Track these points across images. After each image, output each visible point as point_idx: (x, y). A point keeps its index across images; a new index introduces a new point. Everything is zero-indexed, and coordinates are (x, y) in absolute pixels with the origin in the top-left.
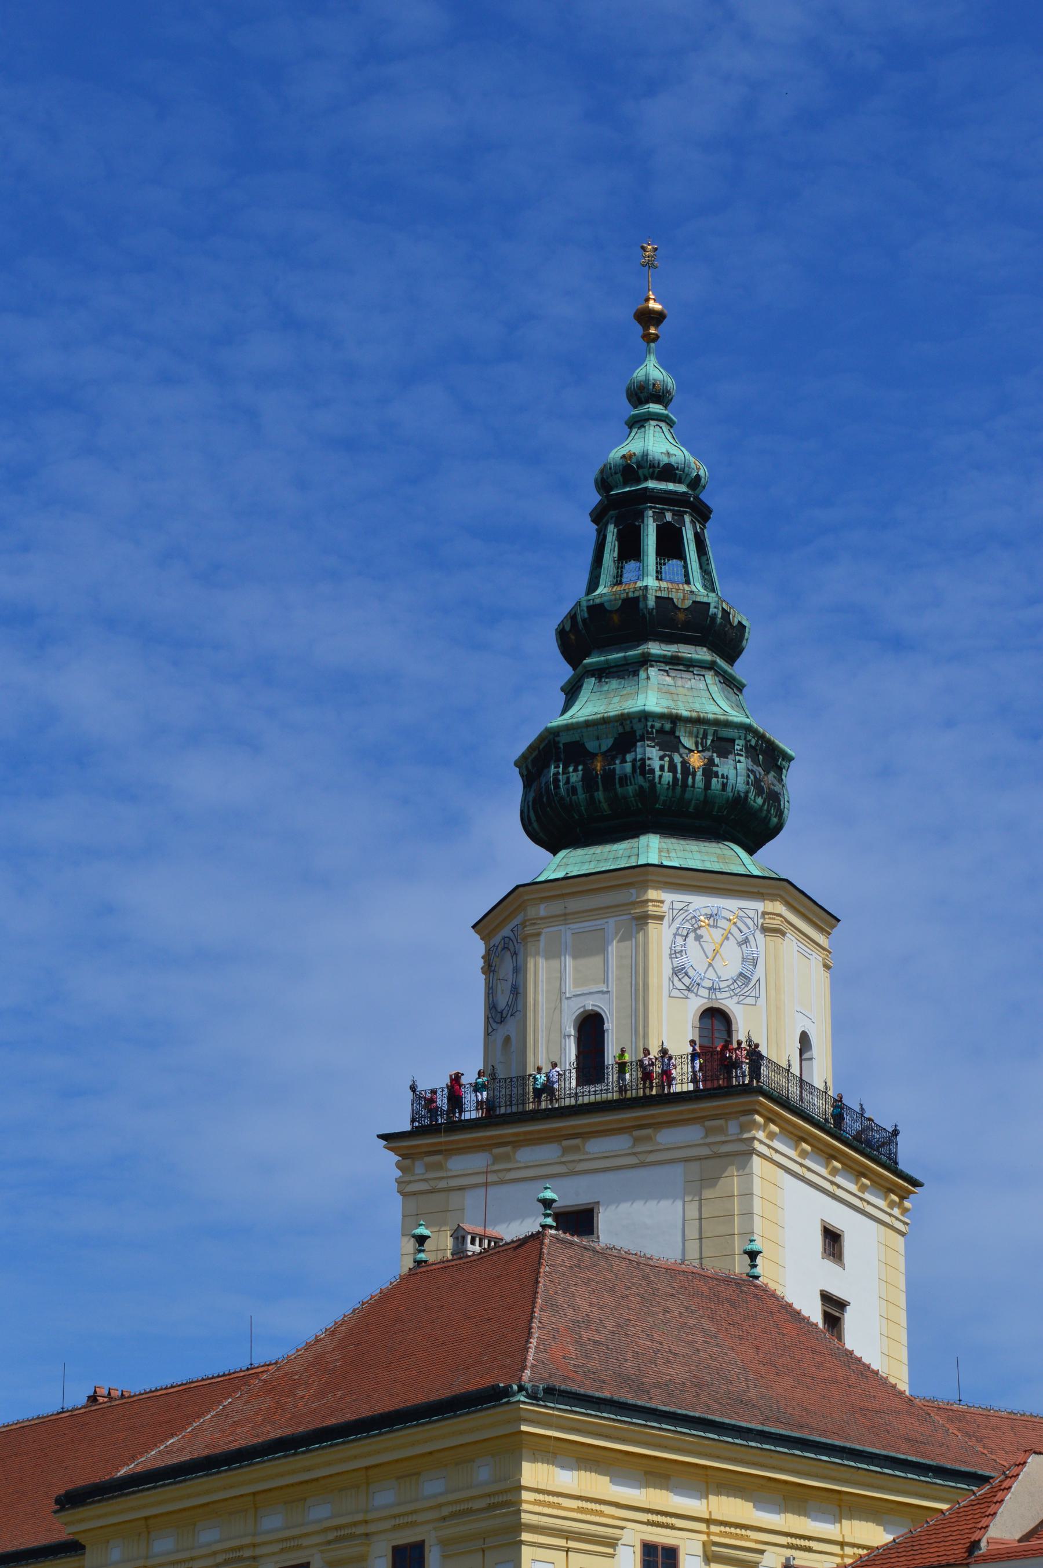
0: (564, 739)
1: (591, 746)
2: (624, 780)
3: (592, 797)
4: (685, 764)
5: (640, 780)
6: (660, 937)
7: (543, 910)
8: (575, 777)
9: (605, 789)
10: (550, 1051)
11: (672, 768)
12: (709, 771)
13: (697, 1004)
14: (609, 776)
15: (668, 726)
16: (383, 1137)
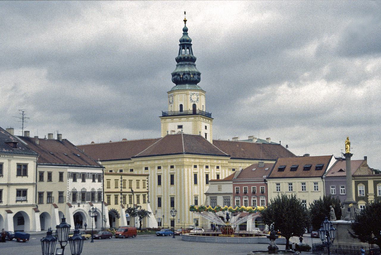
0: (177, 73)
1: (180, 74)
2: (184, 78)
4: (191, 77)
5: (186, 79)
6: (189, 96)
8: (179, 78)
11: (189, 77)
12: (193, 77)
13: (193, 103)
16: (160, 117)
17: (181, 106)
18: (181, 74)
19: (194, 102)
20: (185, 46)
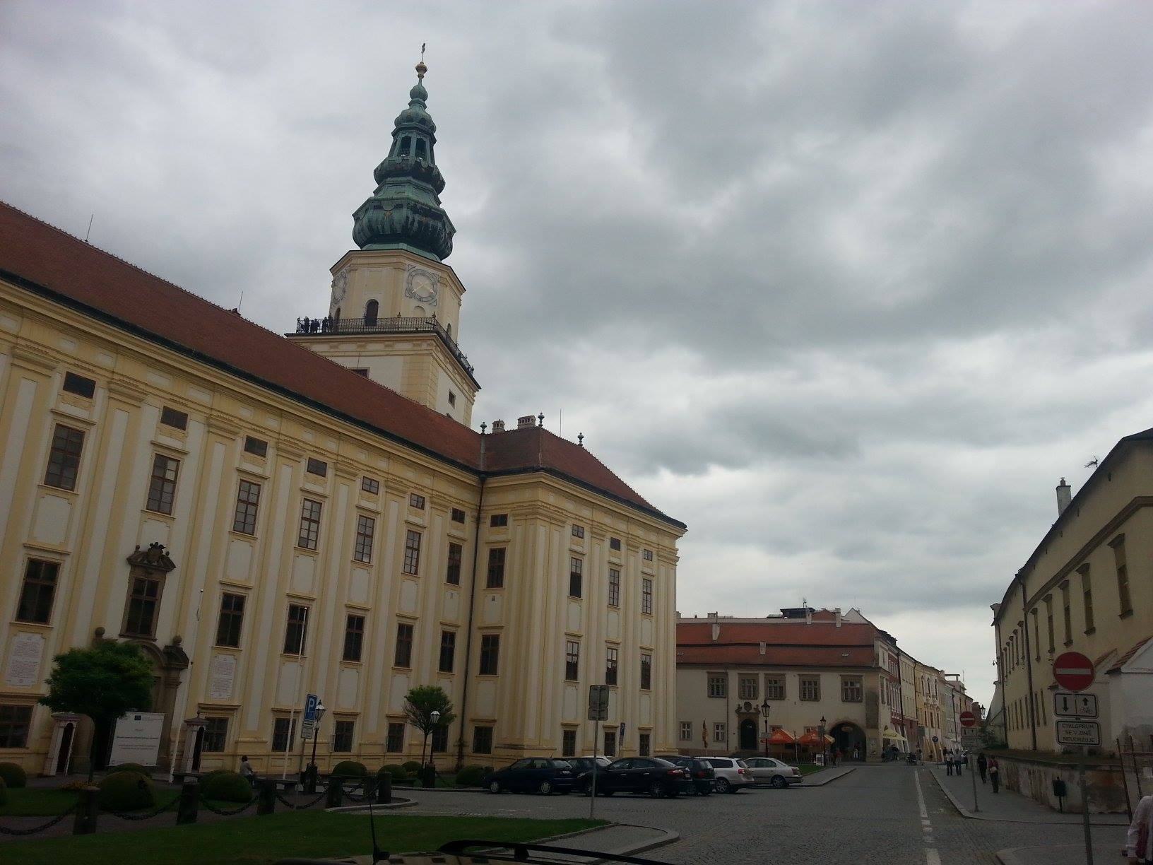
10: (355, 311)
17: (373, 305)
19: (420, 299)
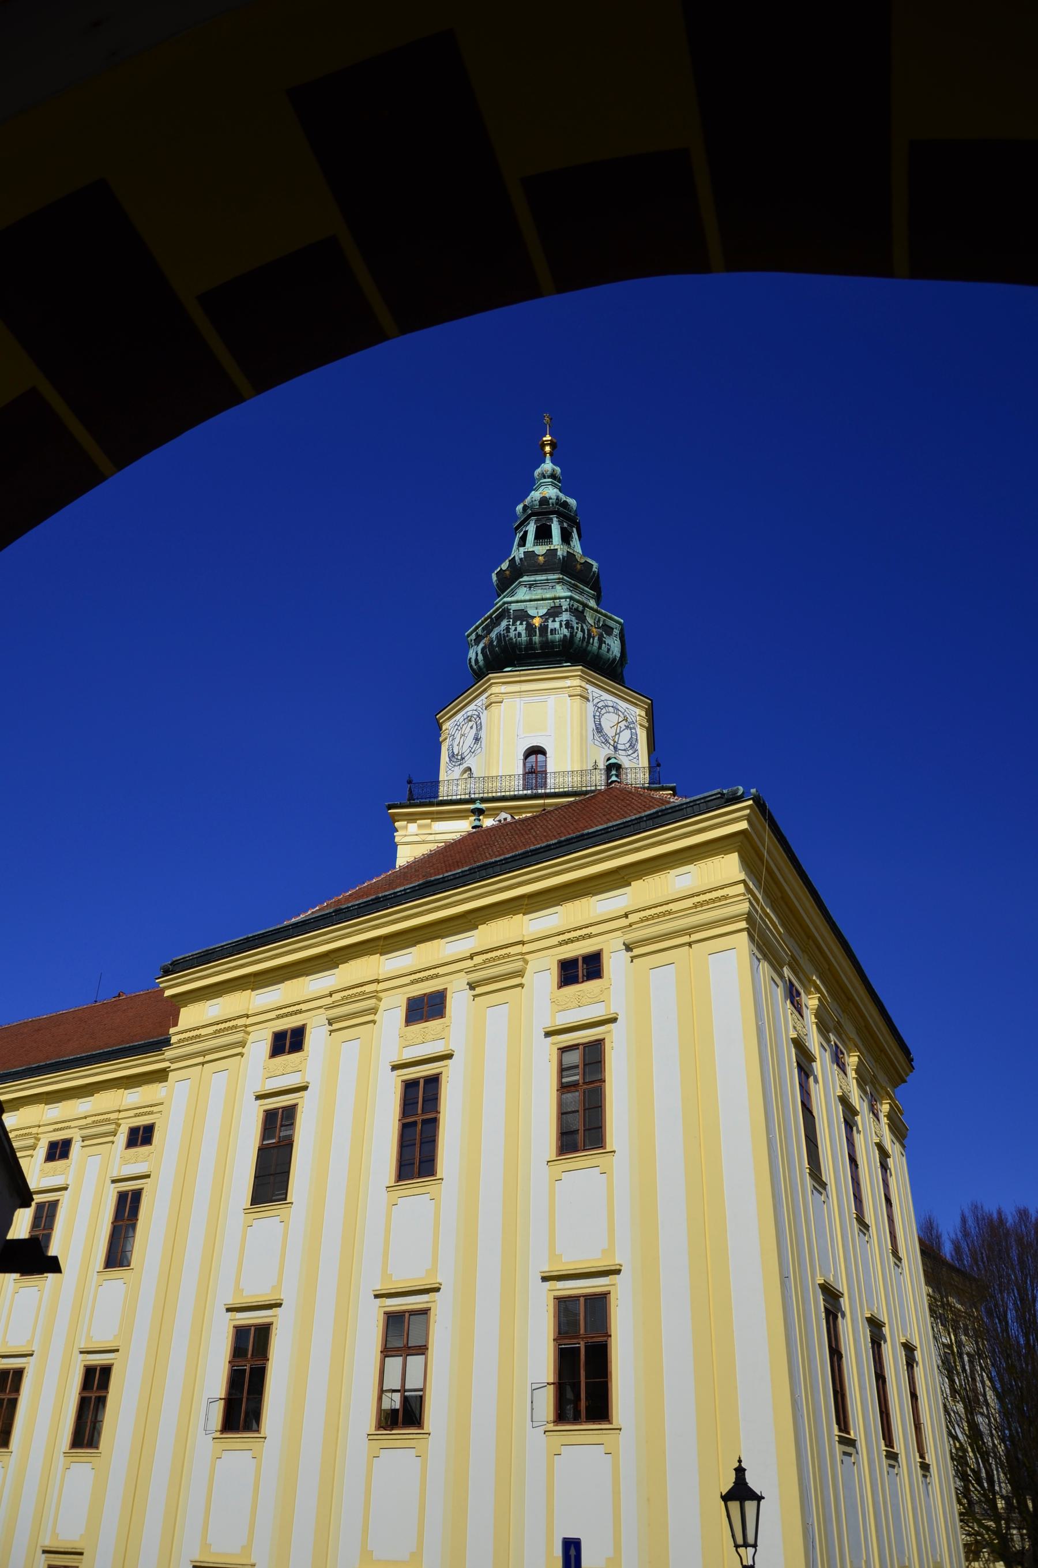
0: (514, 607)
1: (531, 612)
2: (553, 631)
3: (531, 640)
5: (565, 631)
7: (503, 689)
8: (521, 628)
9: (540, 635)
11: (583, 630)
14: (544, 628)
15: (581, 608)
18: (537, 612)
20: (551, 520)
